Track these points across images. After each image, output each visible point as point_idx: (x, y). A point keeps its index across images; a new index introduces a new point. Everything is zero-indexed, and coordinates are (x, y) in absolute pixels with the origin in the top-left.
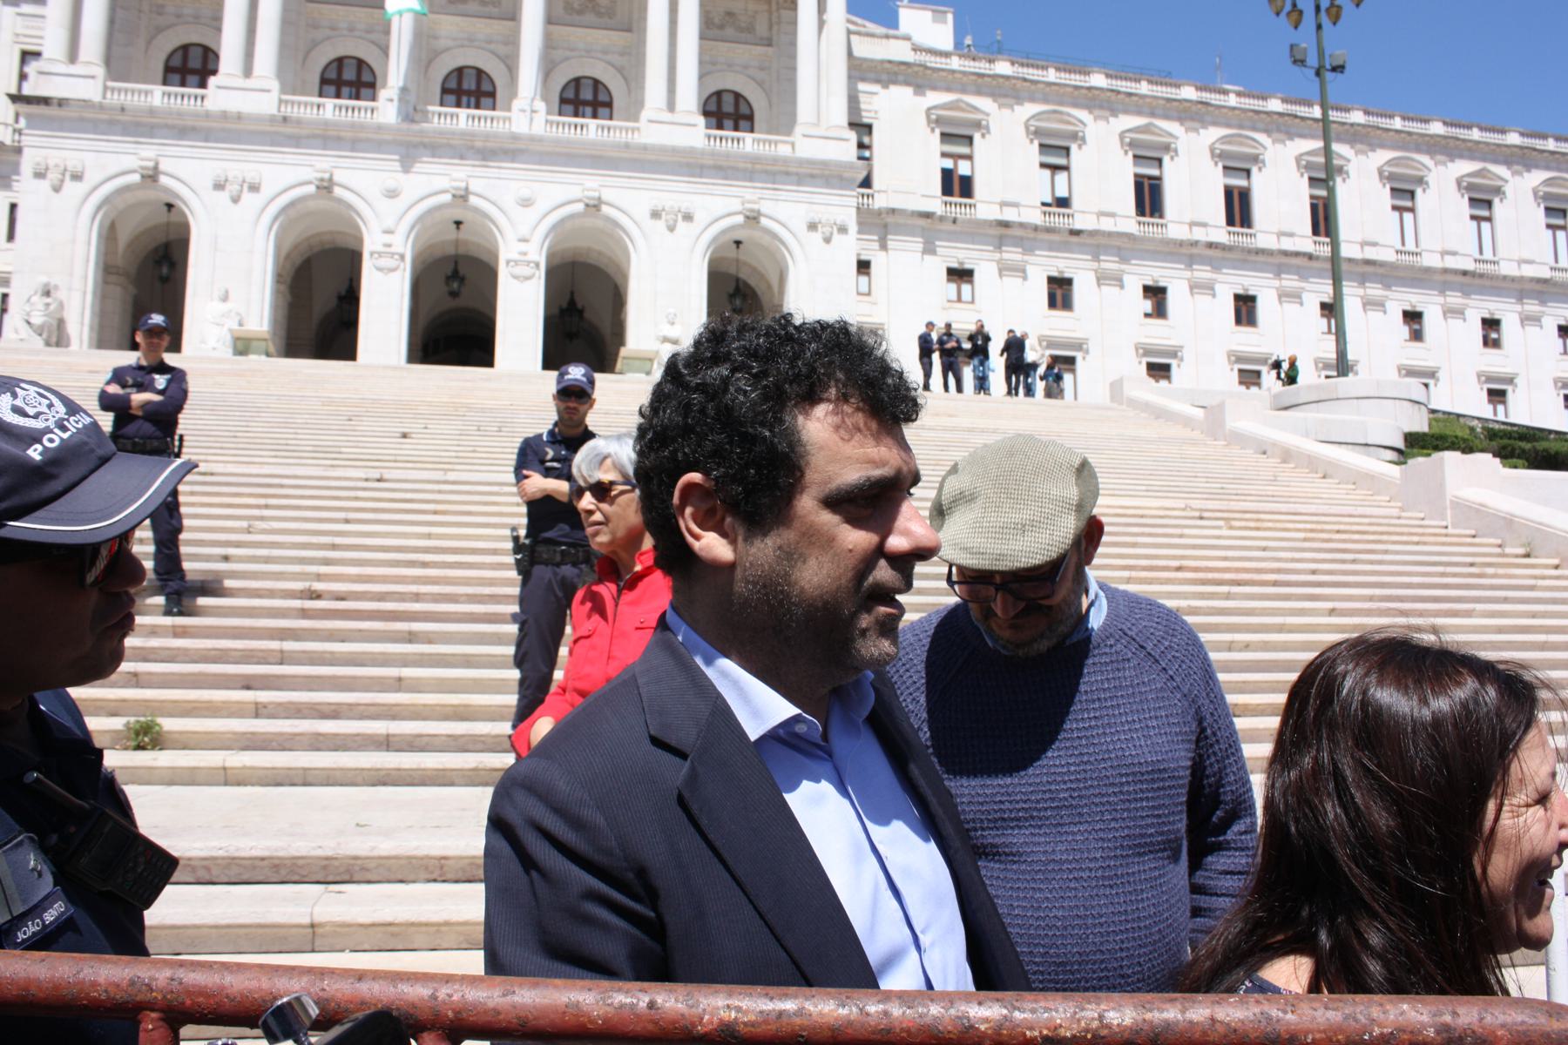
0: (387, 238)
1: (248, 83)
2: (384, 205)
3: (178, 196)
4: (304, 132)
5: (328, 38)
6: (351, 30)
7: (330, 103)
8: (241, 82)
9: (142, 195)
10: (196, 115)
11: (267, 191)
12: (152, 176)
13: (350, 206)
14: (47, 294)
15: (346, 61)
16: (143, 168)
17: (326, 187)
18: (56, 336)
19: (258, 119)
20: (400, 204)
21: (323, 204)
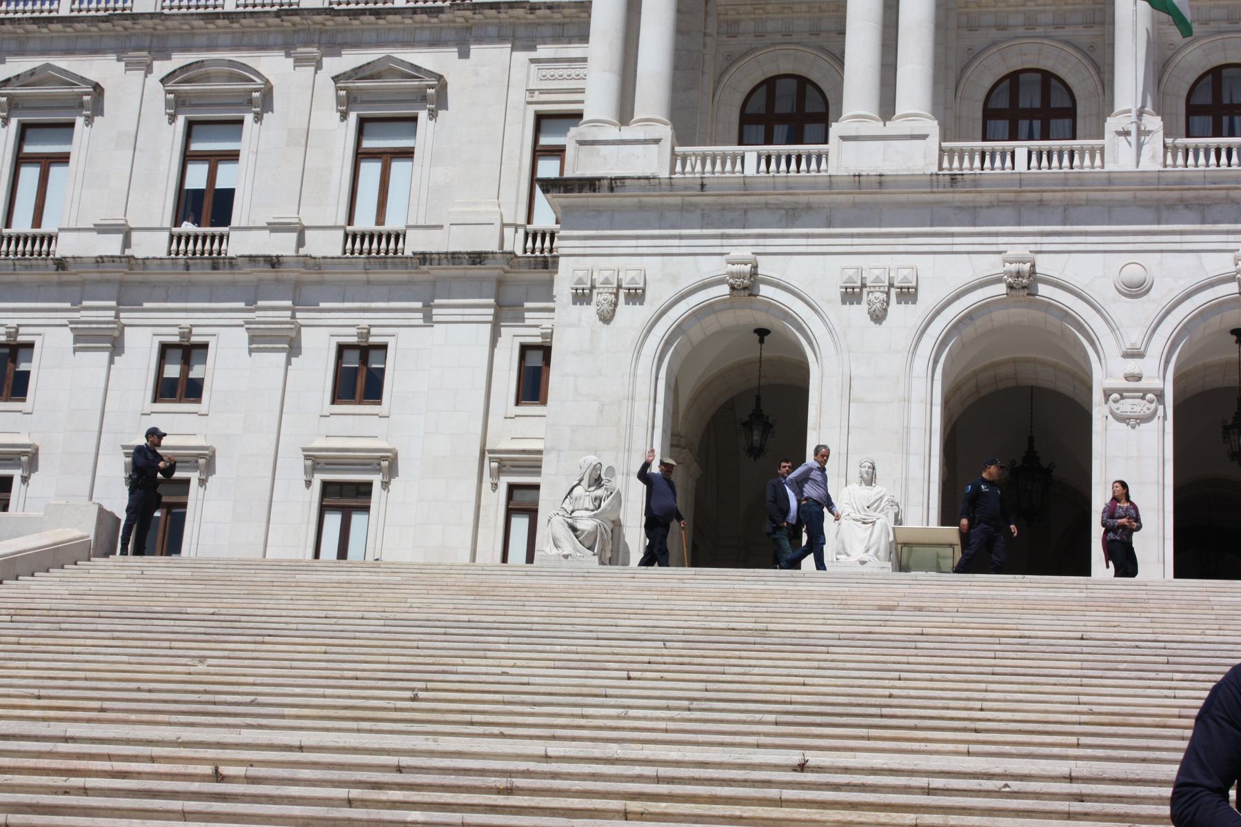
0: (1133, 366)
1: (888, 128)
2: (1121, 309)
3: (787, 316)
4: (986, 198)
5: (994, 44)
6: (1030, 25)
7: (1021, 148)
8: (877, 127)
9: (727, 319)
10: (814, 186)
11: (928, 298)
12: (746, 287)
13: (1066, 315)
14: (597, 482)
15: (1023, 77)
16: (733, 275)
17: (1024, 285)
18: (608, 547)
19: (909, 182)
20: (1150, 306)
21: (1019, 314)
